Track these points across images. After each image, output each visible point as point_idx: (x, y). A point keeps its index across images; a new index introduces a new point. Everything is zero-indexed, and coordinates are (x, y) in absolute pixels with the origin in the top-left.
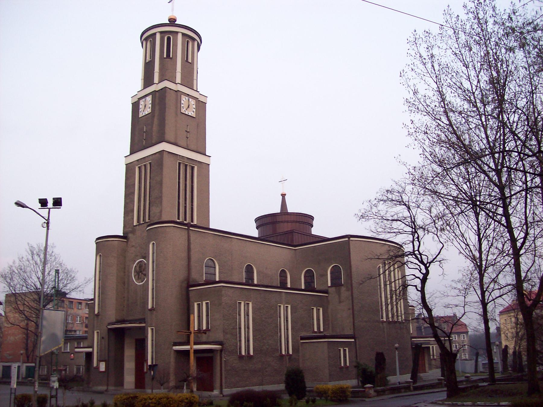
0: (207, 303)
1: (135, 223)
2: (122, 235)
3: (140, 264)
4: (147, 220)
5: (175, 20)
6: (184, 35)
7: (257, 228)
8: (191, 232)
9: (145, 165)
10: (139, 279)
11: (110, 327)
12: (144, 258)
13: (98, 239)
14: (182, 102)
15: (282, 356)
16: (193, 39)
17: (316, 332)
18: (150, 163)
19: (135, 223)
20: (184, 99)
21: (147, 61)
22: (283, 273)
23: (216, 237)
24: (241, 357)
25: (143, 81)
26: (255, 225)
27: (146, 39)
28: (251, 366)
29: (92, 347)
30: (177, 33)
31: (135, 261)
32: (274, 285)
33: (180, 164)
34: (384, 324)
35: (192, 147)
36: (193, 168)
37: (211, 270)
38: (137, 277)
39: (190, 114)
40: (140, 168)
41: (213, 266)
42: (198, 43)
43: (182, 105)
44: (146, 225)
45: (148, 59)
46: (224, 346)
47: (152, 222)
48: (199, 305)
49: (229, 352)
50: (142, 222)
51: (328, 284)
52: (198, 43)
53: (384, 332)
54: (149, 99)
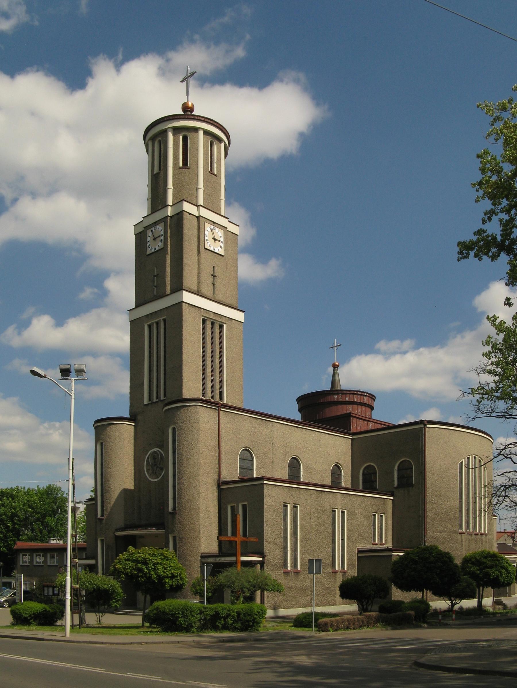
0: (244, 507)
1: (146, 402)
2: (129, 416)
3: (154, 456)
4: (162, 398)
5: (192, 109)
6: (207, 133)
7: (300, 410)
8: (221, 412)
9: (157, 323)
10: (155, 474)
11: (118, 534)
12: (161, 446)
13: (97, 421)
14: (206, 233)
15: (335, 572)
16: (220, 140)
17: (376, 544)
18: (164, 320)
19: (146, 402)
20: (208, 227)
21: (155, 173)
22: (337, 470)
23: (254, 420)
24: (286, 573)
25: (150, 200)
26: (296, 406)
27: (153, 139)
28: (298, 583)
29: (95, 557)
30: (196, 130)
31: (148, 451)
32: (325, 483)
33: (204, 321)
34: (464, 536)
35: (220, 297)
36: (221, 327)
37: (247, 464)
38: (150, 471)
39: (216, 251)
40: (150, 327)
41: (250, 458)
42: (225, 144)
43: (206, 238)
44: (161, 405)
45: (156, 170)
46: (266, 558)
47: (169, 400)
48: (233, 508)
49: (272, 565)
50: (162, 398)
51: (394, 485)
52: (225, 144)
53: (462, 545)
54: (160, 228)
